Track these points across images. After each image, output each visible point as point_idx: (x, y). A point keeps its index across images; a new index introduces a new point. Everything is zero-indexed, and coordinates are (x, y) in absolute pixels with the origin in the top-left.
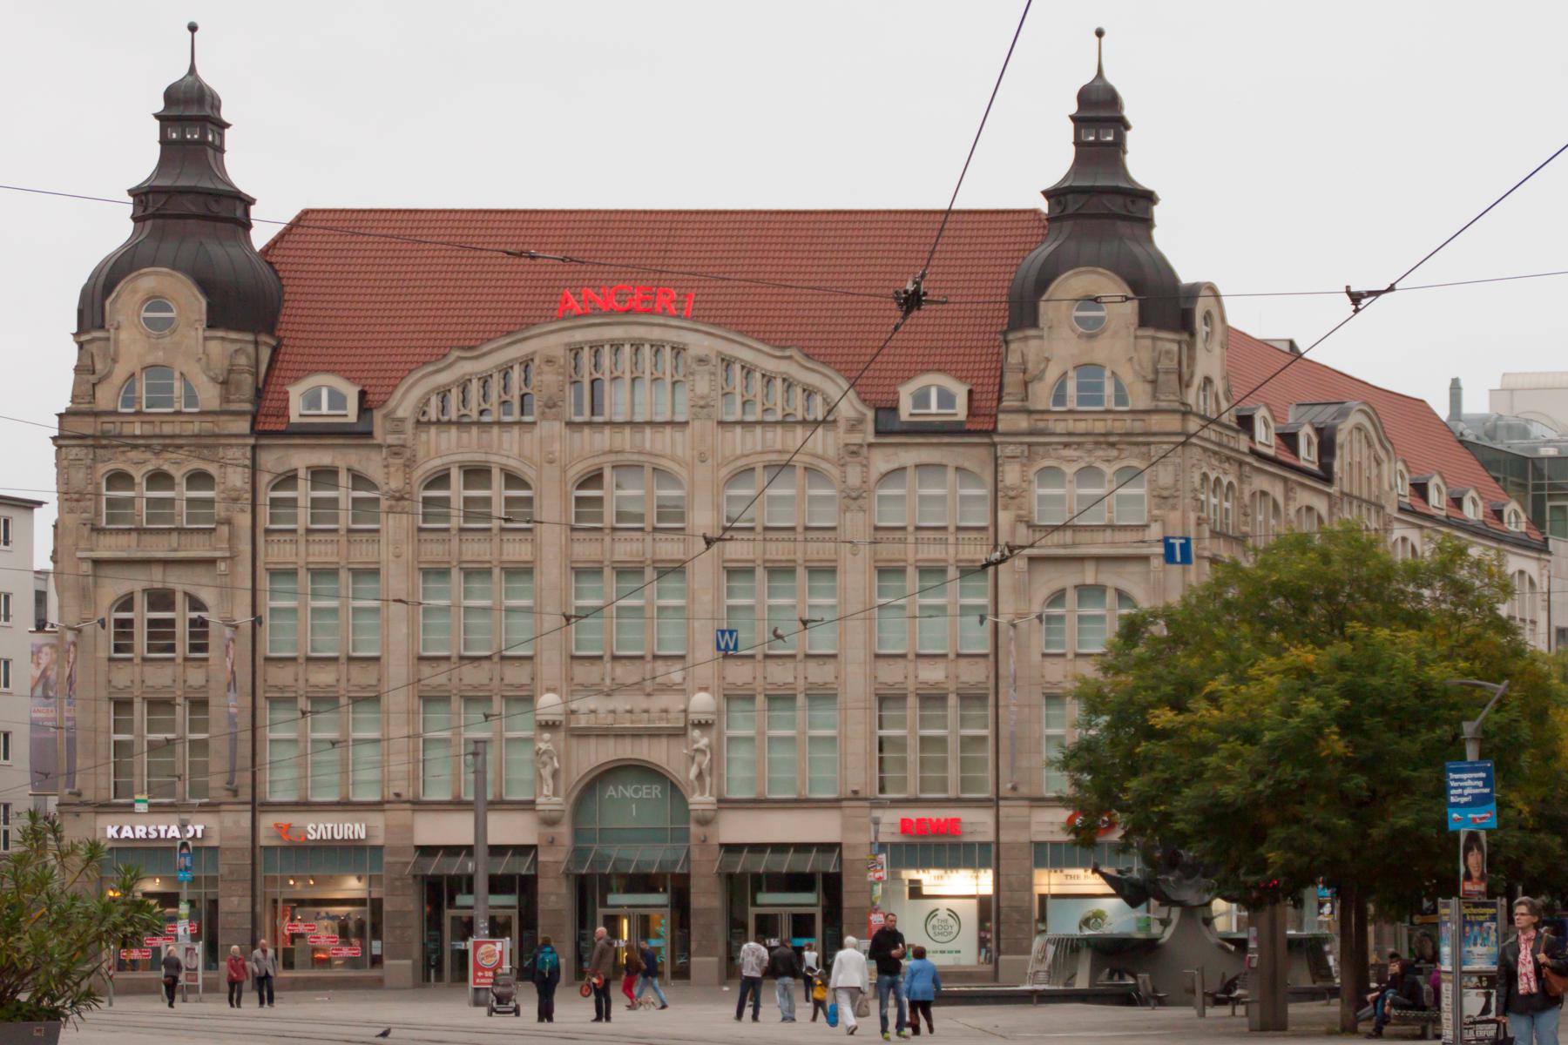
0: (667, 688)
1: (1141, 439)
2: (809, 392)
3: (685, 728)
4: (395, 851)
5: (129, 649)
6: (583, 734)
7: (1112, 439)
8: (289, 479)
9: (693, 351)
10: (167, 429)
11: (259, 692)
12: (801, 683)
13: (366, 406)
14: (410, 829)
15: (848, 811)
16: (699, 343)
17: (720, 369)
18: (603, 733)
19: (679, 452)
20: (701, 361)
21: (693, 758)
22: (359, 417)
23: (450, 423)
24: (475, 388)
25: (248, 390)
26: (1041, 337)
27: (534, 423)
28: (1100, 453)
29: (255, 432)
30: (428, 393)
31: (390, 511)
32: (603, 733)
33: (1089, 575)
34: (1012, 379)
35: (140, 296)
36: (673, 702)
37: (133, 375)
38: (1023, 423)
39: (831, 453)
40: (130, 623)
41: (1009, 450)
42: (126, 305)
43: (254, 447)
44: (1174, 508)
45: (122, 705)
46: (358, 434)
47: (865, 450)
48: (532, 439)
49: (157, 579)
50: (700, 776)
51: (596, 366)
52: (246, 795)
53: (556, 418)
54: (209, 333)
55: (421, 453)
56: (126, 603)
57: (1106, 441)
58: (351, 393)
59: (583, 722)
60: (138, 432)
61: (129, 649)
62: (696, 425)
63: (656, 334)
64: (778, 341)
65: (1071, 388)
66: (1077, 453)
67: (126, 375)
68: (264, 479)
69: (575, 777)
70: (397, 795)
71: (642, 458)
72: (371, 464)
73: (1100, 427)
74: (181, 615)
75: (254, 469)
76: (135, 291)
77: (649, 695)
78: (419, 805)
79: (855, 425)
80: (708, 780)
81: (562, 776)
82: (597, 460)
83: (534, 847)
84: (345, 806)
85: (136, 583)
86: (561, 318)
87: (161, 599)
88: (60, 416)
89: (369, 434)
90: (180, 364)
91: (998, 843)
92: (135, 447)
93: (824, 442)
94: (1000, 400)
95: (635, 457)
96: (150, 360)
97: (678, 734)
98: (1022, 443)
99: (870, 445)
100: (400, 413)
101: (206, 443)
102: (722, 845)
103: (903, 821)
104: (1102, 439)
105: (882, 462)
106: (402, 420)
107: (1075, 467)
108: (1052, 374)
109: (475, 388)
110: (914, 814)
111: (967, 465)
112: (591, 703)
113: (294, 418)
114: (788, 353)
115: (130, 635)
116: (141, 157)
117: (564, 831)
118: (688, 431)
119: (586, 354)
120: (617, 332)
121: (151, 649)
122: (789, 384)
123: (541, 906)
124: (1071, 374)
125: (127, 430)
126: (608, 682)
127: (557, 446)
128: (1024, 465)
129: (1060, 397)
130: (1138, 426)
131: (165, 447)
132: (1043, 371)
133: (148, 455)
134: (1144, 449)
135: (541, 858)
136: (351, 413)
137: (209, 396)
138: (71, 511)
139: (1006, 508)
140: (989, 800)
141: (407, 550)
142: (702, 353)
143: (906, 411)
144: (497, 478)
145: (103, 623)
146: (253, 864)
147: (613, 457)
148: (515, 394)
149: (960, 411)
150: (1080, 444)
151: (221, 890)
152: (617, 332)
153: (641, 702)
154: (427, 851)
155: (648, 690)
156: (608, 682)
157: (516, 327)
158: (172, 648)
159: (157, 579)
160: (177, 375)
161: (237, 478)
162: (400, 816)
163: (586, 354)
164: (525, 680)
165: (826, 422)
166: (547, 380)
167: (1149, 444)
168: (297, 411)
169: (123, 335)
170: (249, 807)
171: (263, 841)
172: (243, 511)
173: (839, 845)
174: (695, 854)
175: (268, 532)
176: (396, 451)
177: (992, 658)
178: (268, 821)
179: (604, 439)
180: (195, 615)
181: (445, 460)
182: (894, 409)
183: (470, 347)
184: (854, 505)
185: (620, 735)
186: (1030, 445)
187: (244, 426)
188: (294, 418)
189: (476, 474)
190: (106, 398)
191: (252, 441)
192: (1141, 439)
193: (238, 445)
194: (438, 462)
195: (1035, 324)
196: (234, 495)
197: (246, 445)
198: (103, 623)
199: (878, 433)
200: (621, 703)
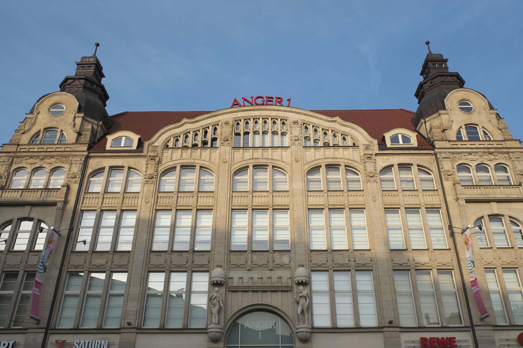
6: (235, 290)
7: (491, 150)
11: (65, 268)
13: (140, 143)
15: (387, 334)
16: (292, 117)
18: (246, 290)
19: (285, 159)
20: (295, 123)
21: (298, 303)
22: (137, 147)
26: (447, 114)
28: (486, 157)
30: (170, 137)
32: (246, 290)
33: (495, 209)
36: (285, 274)
39: (357, 159)
41: (444, 155)
47: (374, 157)
48: (215, 154)
50: (303, 311)
52: (44, 324)
55: (164, 162)
58: (135, 138)
59: (236, 283)
63: (274, 113)
66: (475, 157)
67: (37, 130)
68: (89, 171)
69: (229, 315)
70: (129, 324)
71: (267, 161)
75: (85, 165)
76: (49, 101)
77: (271, 270)
78: (140, 330)
79: (367, 148)
90: (61, 127)
95: (264, 161)
97: (286, 290)
99: (376, 154)
100: (156, 144)
103: (422, 339)
104: (486, 150)
105: (382, 162)
106: (157, 147)
108: (455, 128)
109: (190, 136)
111: (422, 164)
114: (334, 119)
118: (289, 150)
120: (257, 113)
124: (464, 127)
128: (452, 161)
131: (45, 157)
132: (451, 126)
133: (37, 160)
134: (507, 155)
139: (447, 180)
141: (152, 200)
143: (389, 144)
152: (257, 113)
153: (268, 274)
155: (270, 267)
160: (59, 130)
161: (76, 169)
163: (242, 123)
166: (224, 131)
169: (40, 116)
172: (75, 182)
176: (153, 158)
177: (453, 250)
179: (248, 154)
181: (174, 162)
186: (453, 153)
187: (85, 148)
191: (86, 153)
192: (505, 150)
194: (171, 163)
195: (444, 108)
200: (255, 274)
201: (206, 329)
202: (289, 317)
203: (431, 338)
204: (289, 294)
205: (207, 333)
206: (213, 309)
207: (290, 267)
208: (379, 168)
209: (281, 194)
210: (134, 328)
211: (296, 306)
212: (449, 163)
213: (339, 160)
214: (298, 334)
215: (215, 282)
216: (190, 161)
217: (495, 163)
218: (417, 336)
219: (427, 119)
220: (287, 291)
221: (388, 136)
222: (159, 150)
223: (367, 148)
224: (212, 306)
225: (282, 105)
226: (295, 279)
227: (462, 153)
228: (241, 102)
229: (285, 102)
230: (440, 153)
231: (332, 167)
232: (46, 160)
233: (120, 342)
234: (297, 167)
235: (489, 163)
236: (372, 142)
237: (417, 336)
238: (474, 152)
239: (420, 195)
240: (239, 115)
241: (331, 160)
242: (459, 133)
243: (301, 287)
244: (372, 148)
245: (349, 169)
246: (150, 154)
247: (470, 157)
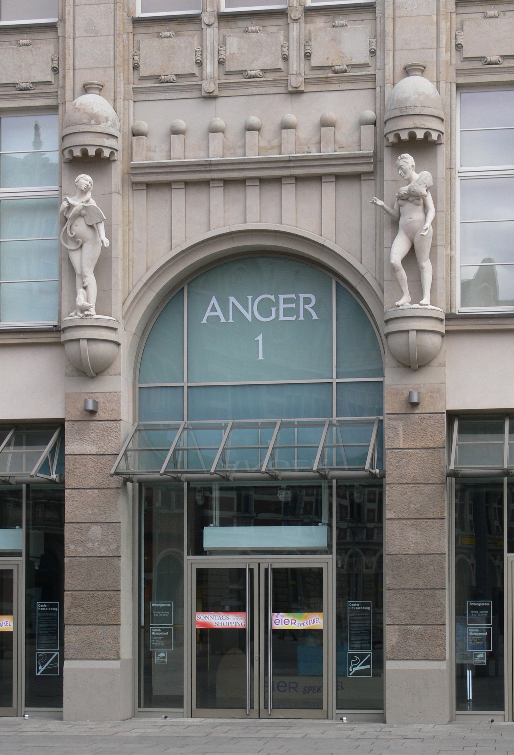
0: (332, 76)
3: (376, 159)
21: (395, 223)
50: (411, 257)
59: (153, 152)
80: (427, 265)
81: (118, 269)
83: (57, 426)
102: (452, 416)
117: (119, 389)
123: (70, 548)
126: (210, 68)
135: (71, 447)
156: (210, 68)
164: (42, 73)
174: (397, 436)
185: (233, 178)
201: (57, 330)
202: (362, 278)
204: (367, 186)
205: (61, 344)
206: (75, 257)
207: (373, 78)
211: (387, 234)
214: (391, 338)
215: (77, 153)
220: (357, 177)
224: (71, 246)
226: (391, 127)
243: (408, 160)
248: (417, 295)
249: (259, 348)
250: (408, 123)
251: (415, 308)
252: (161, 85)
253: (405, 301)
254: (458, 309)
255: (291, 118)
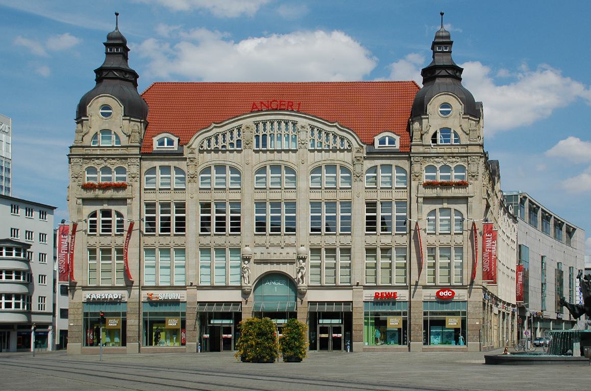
0: (288, 245)
1: (465, 155)
2: (342, 139)
4: (190, 303)
5: (95, 231)
6: (258, 262)
8: (152, 170)
9: (298, 126)
10: (109, 152)
12: (338, 244)
13: (181, 145)
14: (196, 295)
16: (302, 121)
17: (310, 130)
18: (265, 262)
23: (211, 150)
24: (220, 137)
25: (138, 139)
26: (428, 118)
27: (242, 150)
28: (449, 160)
29: (140, 153)
31: (190, 181)
32: (265, 262)
34: (416, 135)
35: (100, 104)
36: (291, 251)
37: (97, 133)
38: (421, 149)
40: (95, 222)
42: (94, 109)
43: (141, 159)
44: (476, 179)
45: (92, 251)
46: (178, 156)
49: (106, 207)
50: (302, 277)
51: (265, 130)
53: (250, 148)
54: (124, 118)
56: (94, 215)
57: (452, 155)
59: (258, 257)
60: (98, 153)
61: (95, 231)
62: (300, 151)
63: (286, 118)
64: (330, 121)
65: (439, 135)
68: (144, 170)
71: (281, 162)
72: (182, 165)
73: (449, 151)
74: (115, 219)
76: (98, 103)
78: (200, 288)
82: (264, 163)
84: (172, 288)
85: (98, 208)
86: (252, 112)
87: (106, 213)
88: (71, 147)
89: (182, 154)
90: (114, 129)
91: (410, 301)
92: (98, 159)
93: (347, 157)
94: (411, 141)
96: (104, 127)
98: (421, 156)
100: (193, 146)
101: (123, 158)
103: (376, 293)
105: (368, 164)
106: (194, 149)
107: (440, 165)
108: (431, 133)
109: (220, 137)
110: (380, 291)
111: (399, 165)
112: (263, 249)
113: (155, 149)
115: (95, 226)
116: (99, 59)
119: (261, 125)
121: (103, 231)
122: (335, 136)
125: (94, 152)
127: (250, 158)
129: (434, 141)
130: (463, 150)
131: (108, 158)
133: (103, 161)
134: (466, 159)
136: (175, 147)
137: (124, 141)
138: (75, 181)
139: (414, 180)
140: (407, 286)
142: (303, 125)
143: (377, 144)
144: (228, 171)
145: (86, 221)
146: (139, 308)
147: (270, 162)
148: (235, 139)
149: (397, 145)
150: (442, 157)
151: (128, 316)
153: (281, 251)
154: (202, 304)
157: (235, 116)
158: (110, 231)
159: (106, 207)
162: (193, 291)
163: (261, 125)
165: (349, 151)
167: (467, 157)
168: (156, 146)
169: (93, 118)
170: (138, 287)
171: (142, 300)
172: (136, 181)
173: (352, 302)
175: (145, 189)
178: (144, 294)
180: (119, 219)
182: (373, 144)
183: (219, 122)
184: (358, 179)
186: (424, 157)
187: (137, 151)
188: (155, 149)
189: (221, 168)
190: (88, 141)
193: (135, 158)
196: (133, 175)
197: (138, 158)
198: (86, 221)
199: (367, 153)
200: (272, 250)
203: (381, 293)
208: (365, 168)
209: (290, 190)
210: (194, 286)
212: (419, 165)
213: (336, 162)
216: (221, 162)
217: (455, 165)
218: (372, 293)
219: (414, 119)
221: (377, 139)
222: (197, 151)
223: (358, 152)
225: (292, 111)
227: (431, 157)
228: (259, 105)
229: (295, 108)
230: (413, 156)
231: (331, 168)
232: (109, 161)
233: (187, 294)
234: (302, 167)
235: (450, 165)
236: (362, 147)
237: (372, 293)
238: (440, 156)
239: (394, 191)
240: (258, 119)
241: (329, 162)
242: (435, 135)
244: (362, 151)
245: (344, 169)
246: (190, 156)
247: (436, 160)
248: (303, 282)
249: (277, 289)
250: (301, 255)
251: (302, 285)
252: (258, 245)
253: (300, 283)
254: (310, 284)
255: (282, 252)
